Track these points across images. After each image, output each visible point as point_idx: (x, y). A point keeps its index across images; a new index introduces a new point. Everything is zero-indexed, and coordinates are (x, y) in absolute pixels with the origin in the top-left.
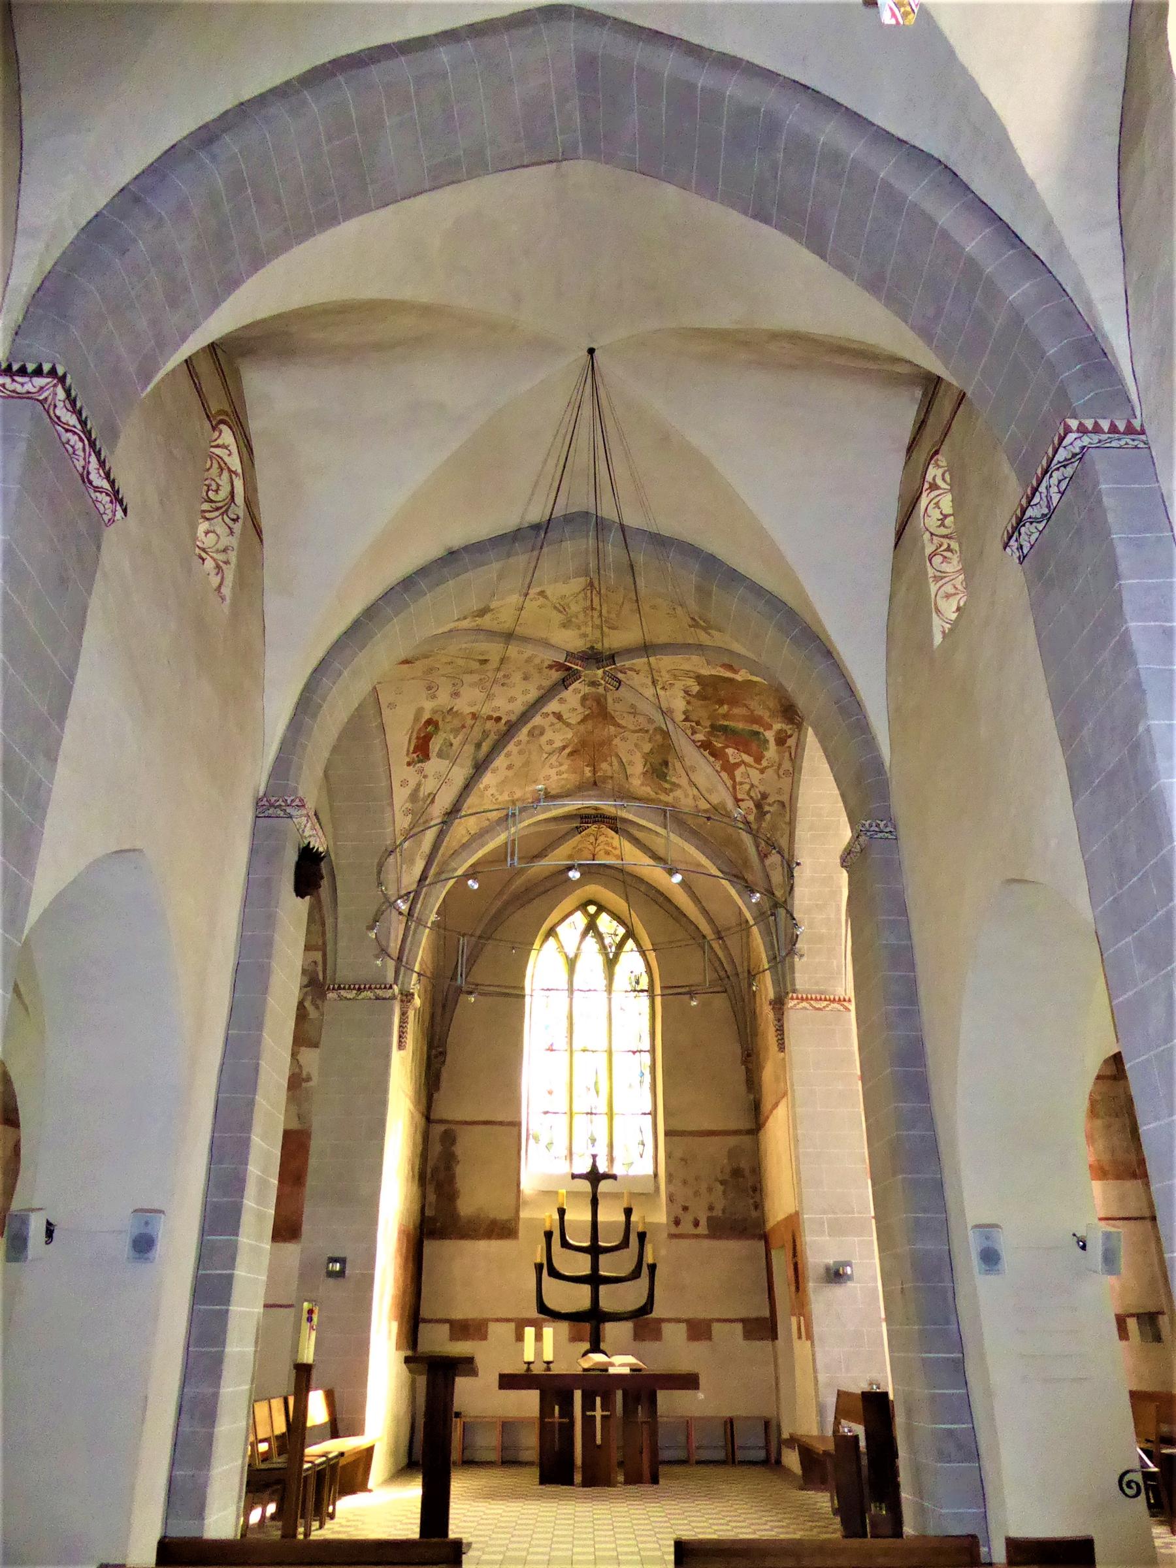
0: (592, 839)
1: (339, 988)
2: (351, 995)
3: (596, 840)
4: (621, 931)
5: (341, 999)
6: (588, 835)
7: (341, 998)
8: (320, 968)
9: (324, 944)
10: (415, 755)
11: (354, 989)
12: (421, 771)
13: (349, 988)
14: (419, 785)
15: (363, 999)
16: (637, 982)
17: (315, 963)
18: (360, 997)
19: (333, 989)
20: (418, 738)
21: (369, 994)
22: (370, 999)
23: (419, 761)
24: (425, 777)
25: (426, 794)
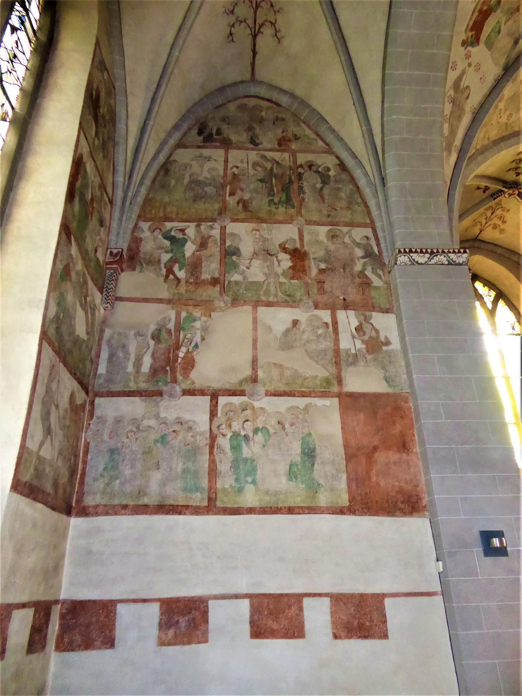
0: (489, 214)
1: (411, 251)
2: (422, 259)
3: (492, 214)
4: (493, 294)
5: (412, 264)
6: (487, 209)
7: (414, 263)
8: (373, 243)
9: (372, 221)
10: (470, 34)
11: (427, 252)
12: (468, 56)
13: (421, 252)
14: (463, 73)
15: (436, 264)
16: (513, 328)
17: (367, 238)
18: (433, 262)
19: (405, 252)
20: (480, 11)
21: (443, 259)
22: (443, 264)
23: (472, 45)
24: (470, 65)
25: (465, 86)
